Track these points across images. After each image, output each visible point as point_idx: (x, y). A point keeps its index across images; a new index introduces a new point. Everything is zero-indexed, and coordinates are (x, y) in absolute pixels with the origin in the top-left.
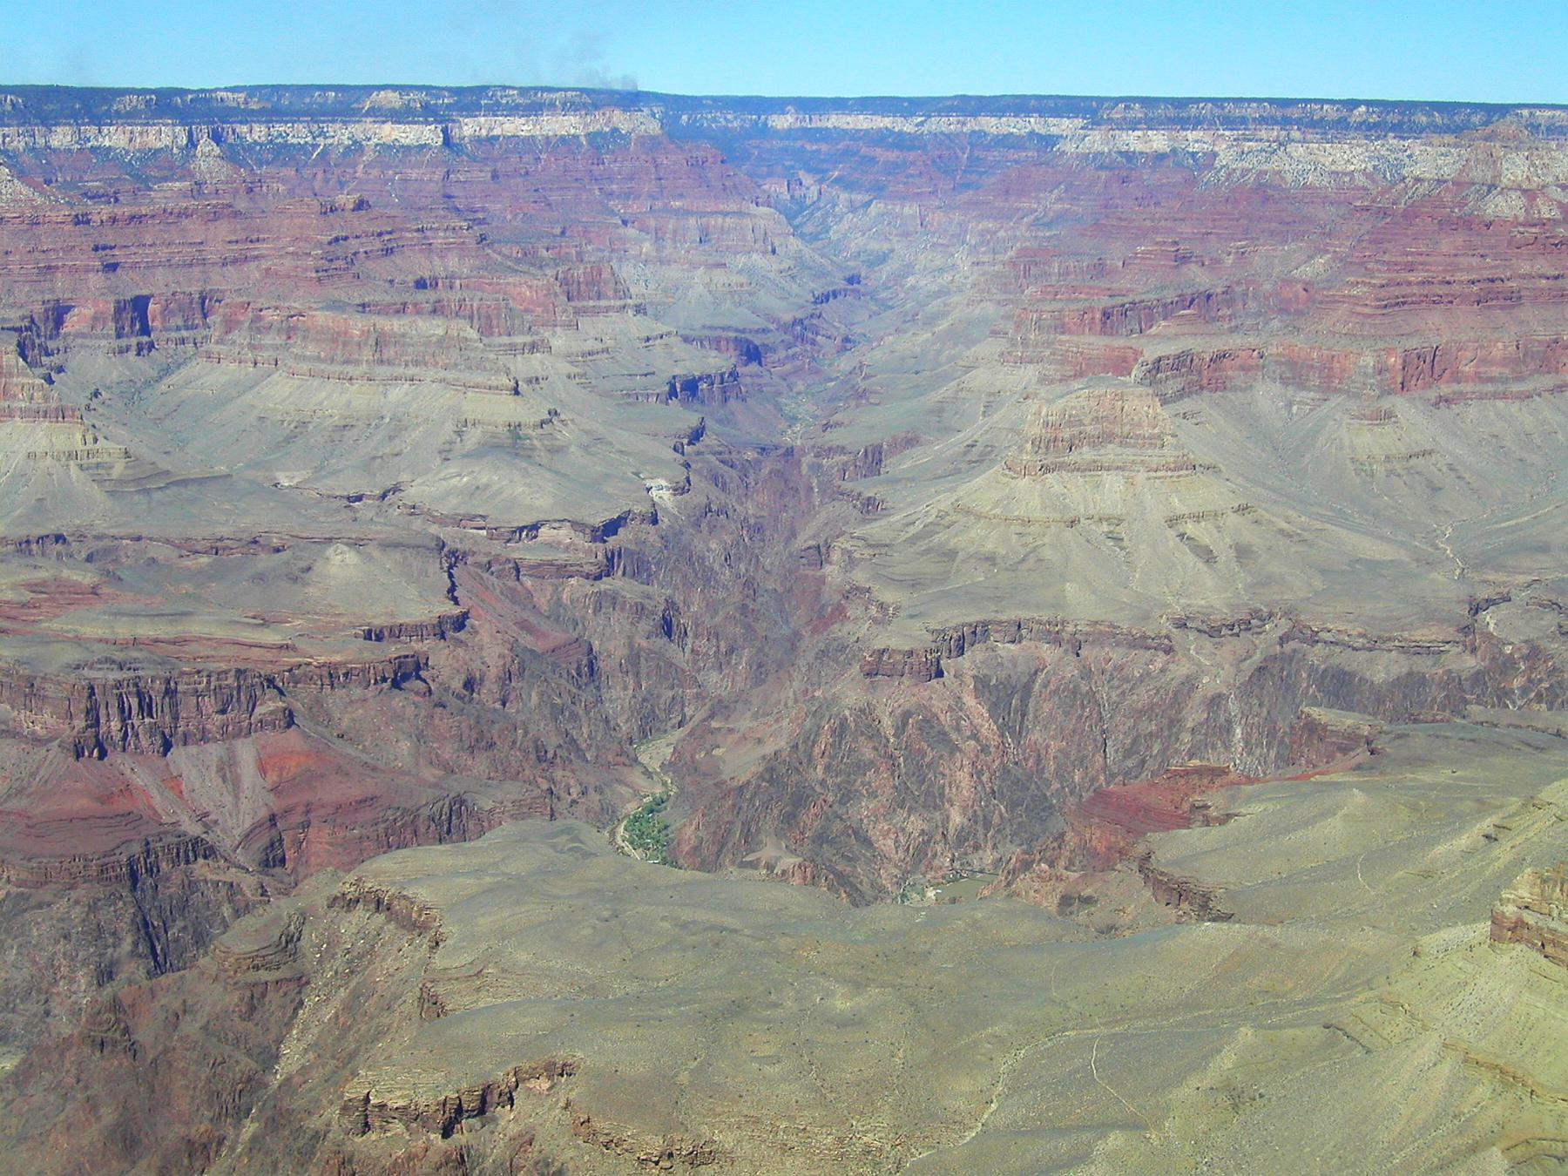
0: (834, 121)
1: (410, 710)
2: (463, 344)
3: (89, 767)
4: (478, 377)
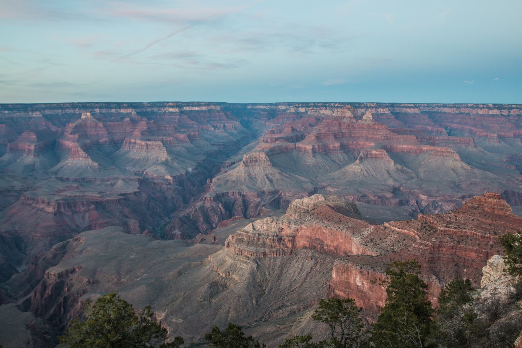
0: (257, 107)
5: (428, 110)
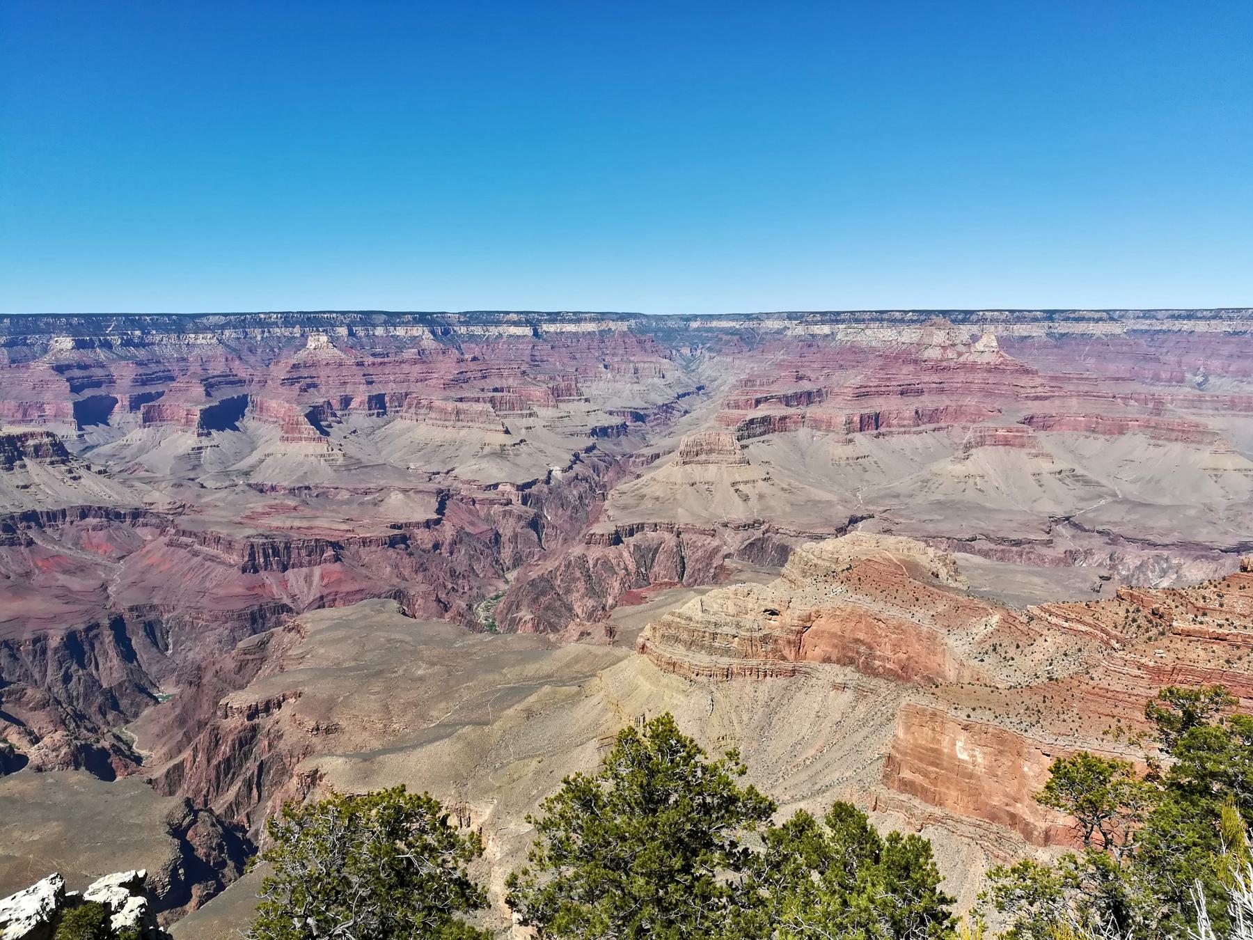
0: (715, 324)
1: (394, 556)
2: (487, 414)
3: (249, 576)
4: (492, 427)
5: (1144, 327)
